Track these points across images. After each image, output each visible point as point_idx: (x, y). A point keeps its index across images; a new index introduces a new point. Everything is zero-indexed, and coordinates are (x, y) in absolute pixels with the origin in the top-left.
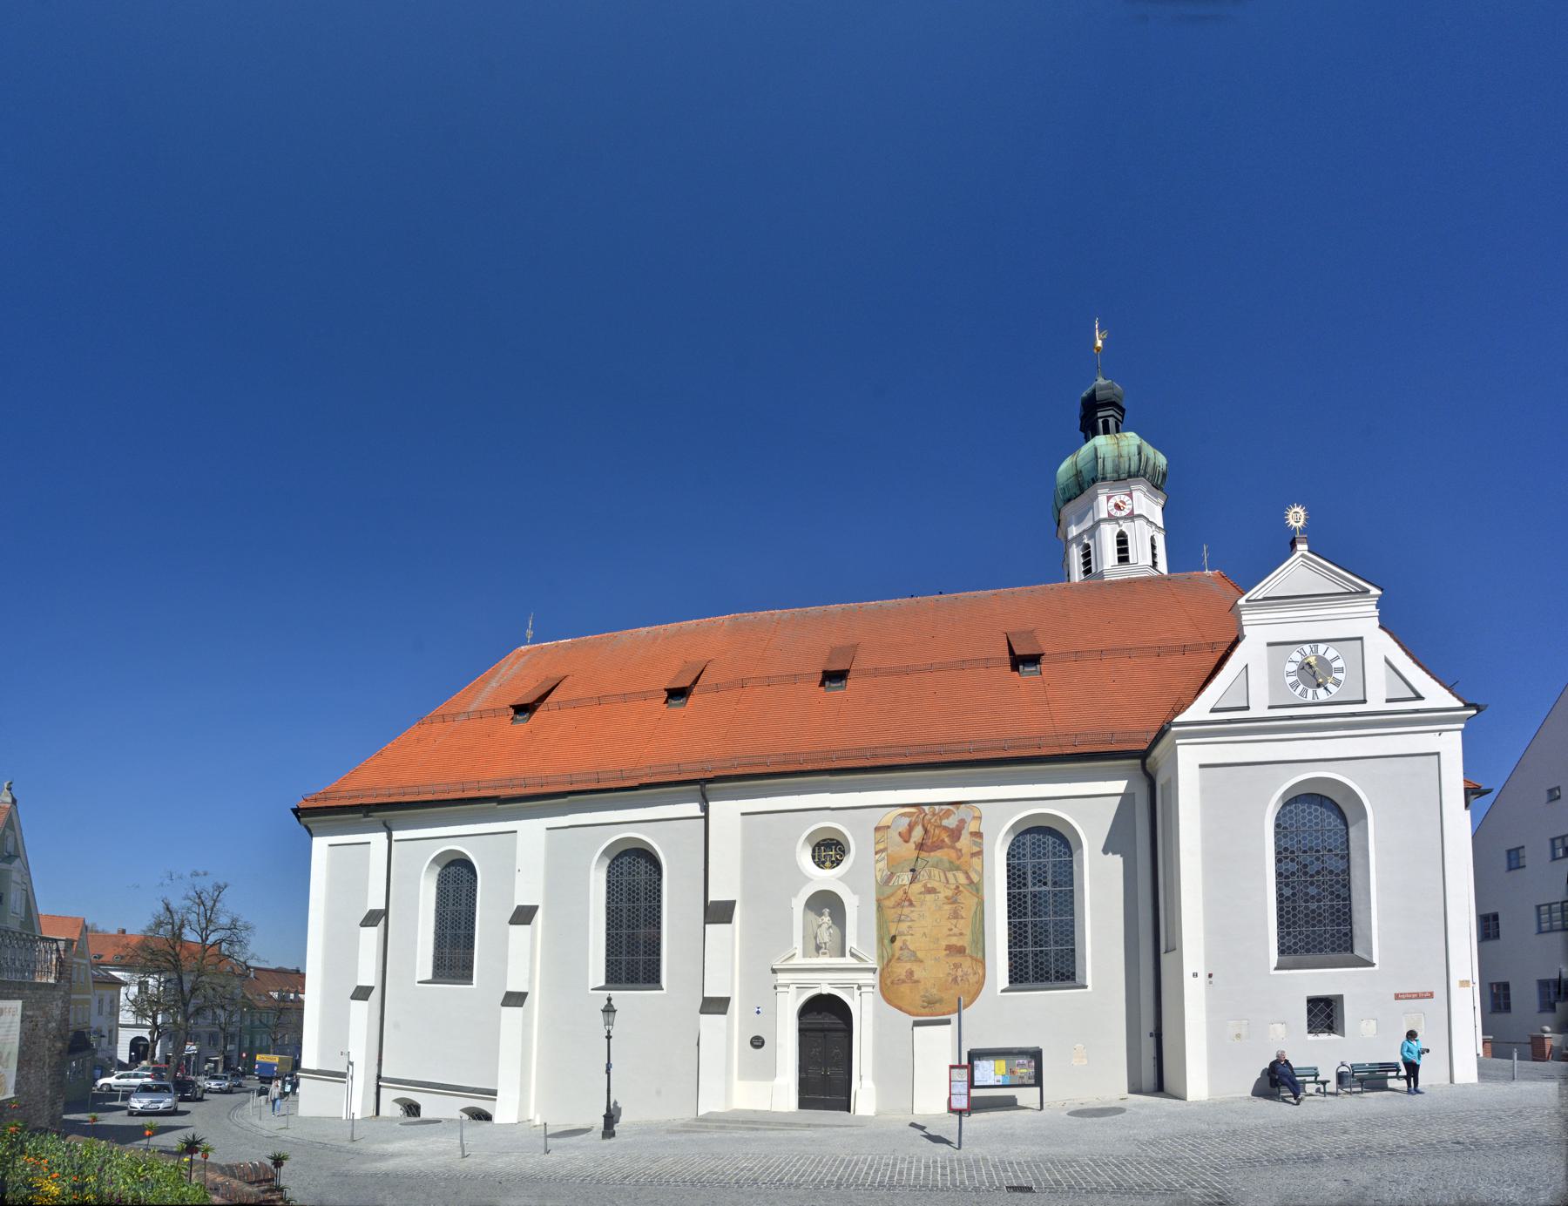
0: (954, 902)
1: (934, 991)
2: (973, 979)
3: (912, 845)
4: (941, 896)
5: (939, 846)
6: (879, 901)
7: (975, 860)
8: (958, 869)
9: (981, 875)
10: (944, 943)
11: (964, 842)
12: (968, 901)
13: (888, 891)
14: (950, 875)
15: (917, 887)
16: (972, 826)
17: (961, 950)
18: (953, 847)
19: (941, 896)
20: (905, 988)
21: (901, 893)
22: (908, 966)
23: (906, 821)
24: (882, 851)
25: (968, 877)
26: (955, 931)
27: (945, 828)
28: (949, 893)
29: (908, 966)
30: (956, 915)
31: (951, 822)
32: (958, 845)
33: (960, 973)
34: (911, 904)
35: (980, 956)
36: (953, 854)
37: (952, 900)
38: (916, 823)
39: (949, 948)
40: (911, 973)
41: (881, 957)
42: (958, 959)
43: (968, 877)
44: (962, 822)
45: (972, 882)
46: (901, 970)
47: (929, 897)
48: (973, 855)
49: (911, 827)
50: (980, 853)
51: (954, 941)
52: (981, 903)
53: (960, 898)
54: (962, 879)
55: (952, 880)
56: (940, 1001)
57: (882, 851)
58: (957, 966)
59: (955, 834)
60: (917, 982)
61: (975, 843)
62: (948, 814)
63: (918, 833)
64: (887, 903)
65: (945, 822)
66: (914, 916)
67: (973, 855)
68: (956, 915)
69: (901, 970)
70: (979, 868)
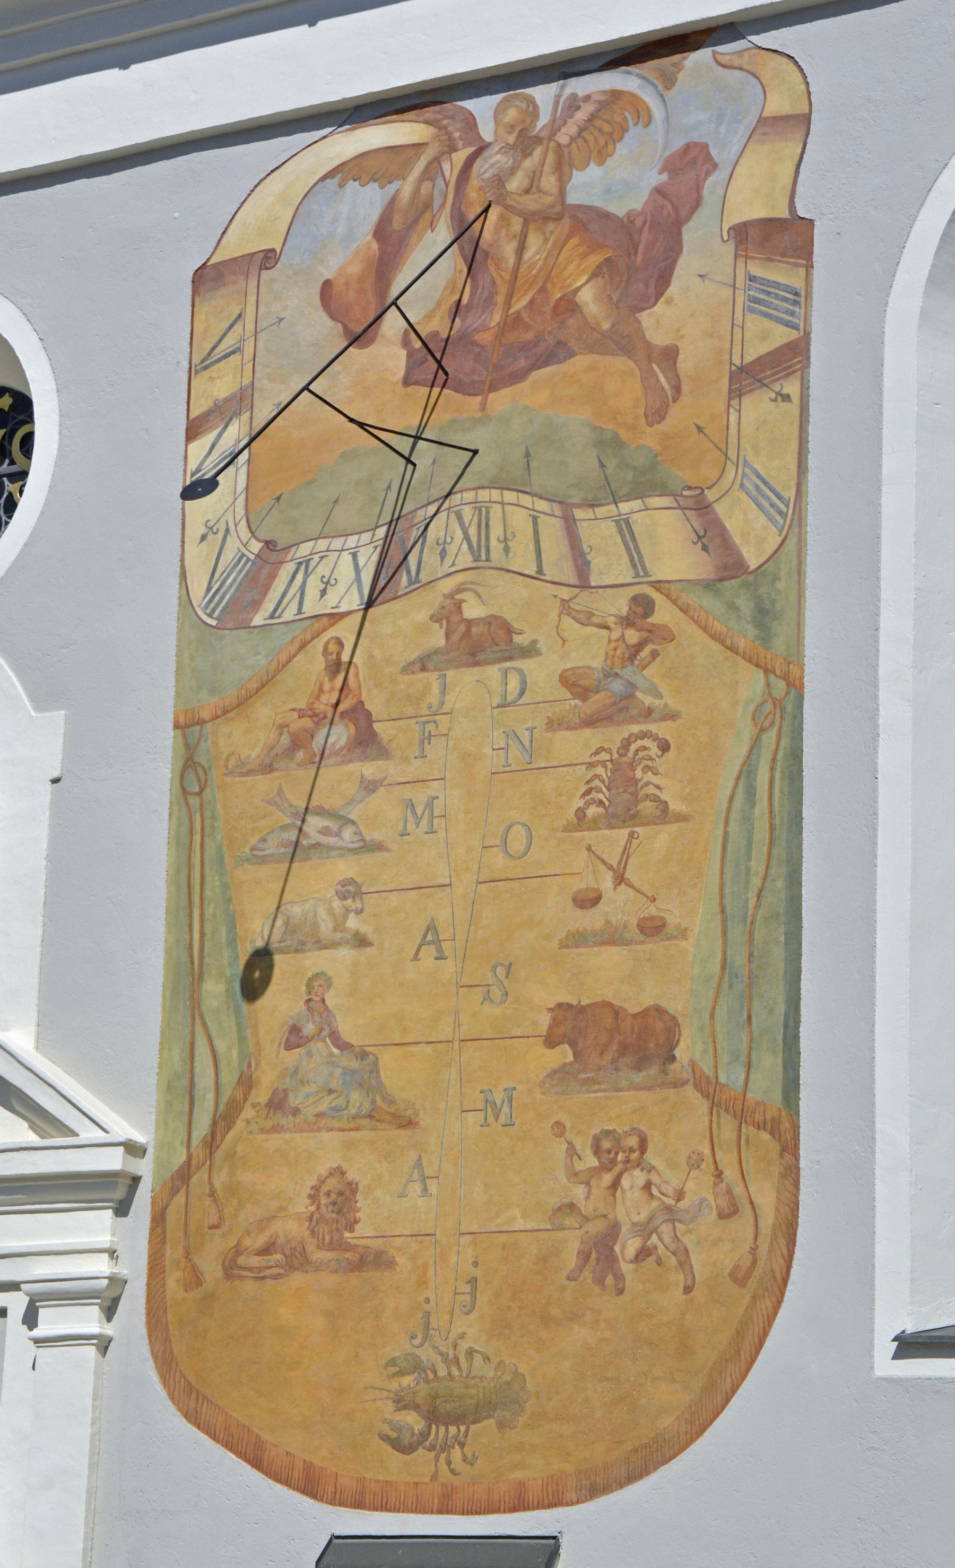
0: (621, 708)
1: (470, 1330)
2: (715, 1249)
3: (389, 354)
4: (541, 673)
5: (537, 346)
6: (187, 725)
7: (757, 408)
8: (646, 484)
9: (792, 516)
10: (544, 993)
11: (699, 303)
12: (704, 689)
13: (244, 657)
14: (597, 530)
15: (407, 624)
18: (626, 342)
19: (541, 673)
20: (298, 1305)
21: (313, 664)
22: (327, 1151)
23: (366, 203)
24: (223, 412)
25: (711, 535)
26: (619, 906)
27: (587, 223)
28: (589, 650)
29: (327, 1151)
30: (623, 800)
31: (617, 182)
32: (657, 324)
33: (632, 1207)
34: (366, 741)
35: (764, 1087)
36: (621, 380)
37: (599, 700)
38: (421, 212)
39: (572, 1025)
40: (339, 1200)
41: (180, 1092)
42: (624, 1105)
43: (711, 535)
44: (691, 162)
45: (731, 567)
46: (281, 1177)
47: (469, 686)
48: (748, 377)
49: (391, 239)
50: (792, 357)
51: (612, 978)
52: (783, 711)
53: (654, 681)
54: (672, 550)
55: (609, 566)
56: (499, 1402)
57: (223, 412)
58: (618, 1155)
59: (642, 252)
60: (372, 1261)
61: (762, 297)
62: (606, 127)
63: (428, 283)
64: (246, 738)
65: (587, 186)
66: (381, 814)
67: (748, 377)
68: (623, 800)
69: (281, 1177)
70: (780, 470)
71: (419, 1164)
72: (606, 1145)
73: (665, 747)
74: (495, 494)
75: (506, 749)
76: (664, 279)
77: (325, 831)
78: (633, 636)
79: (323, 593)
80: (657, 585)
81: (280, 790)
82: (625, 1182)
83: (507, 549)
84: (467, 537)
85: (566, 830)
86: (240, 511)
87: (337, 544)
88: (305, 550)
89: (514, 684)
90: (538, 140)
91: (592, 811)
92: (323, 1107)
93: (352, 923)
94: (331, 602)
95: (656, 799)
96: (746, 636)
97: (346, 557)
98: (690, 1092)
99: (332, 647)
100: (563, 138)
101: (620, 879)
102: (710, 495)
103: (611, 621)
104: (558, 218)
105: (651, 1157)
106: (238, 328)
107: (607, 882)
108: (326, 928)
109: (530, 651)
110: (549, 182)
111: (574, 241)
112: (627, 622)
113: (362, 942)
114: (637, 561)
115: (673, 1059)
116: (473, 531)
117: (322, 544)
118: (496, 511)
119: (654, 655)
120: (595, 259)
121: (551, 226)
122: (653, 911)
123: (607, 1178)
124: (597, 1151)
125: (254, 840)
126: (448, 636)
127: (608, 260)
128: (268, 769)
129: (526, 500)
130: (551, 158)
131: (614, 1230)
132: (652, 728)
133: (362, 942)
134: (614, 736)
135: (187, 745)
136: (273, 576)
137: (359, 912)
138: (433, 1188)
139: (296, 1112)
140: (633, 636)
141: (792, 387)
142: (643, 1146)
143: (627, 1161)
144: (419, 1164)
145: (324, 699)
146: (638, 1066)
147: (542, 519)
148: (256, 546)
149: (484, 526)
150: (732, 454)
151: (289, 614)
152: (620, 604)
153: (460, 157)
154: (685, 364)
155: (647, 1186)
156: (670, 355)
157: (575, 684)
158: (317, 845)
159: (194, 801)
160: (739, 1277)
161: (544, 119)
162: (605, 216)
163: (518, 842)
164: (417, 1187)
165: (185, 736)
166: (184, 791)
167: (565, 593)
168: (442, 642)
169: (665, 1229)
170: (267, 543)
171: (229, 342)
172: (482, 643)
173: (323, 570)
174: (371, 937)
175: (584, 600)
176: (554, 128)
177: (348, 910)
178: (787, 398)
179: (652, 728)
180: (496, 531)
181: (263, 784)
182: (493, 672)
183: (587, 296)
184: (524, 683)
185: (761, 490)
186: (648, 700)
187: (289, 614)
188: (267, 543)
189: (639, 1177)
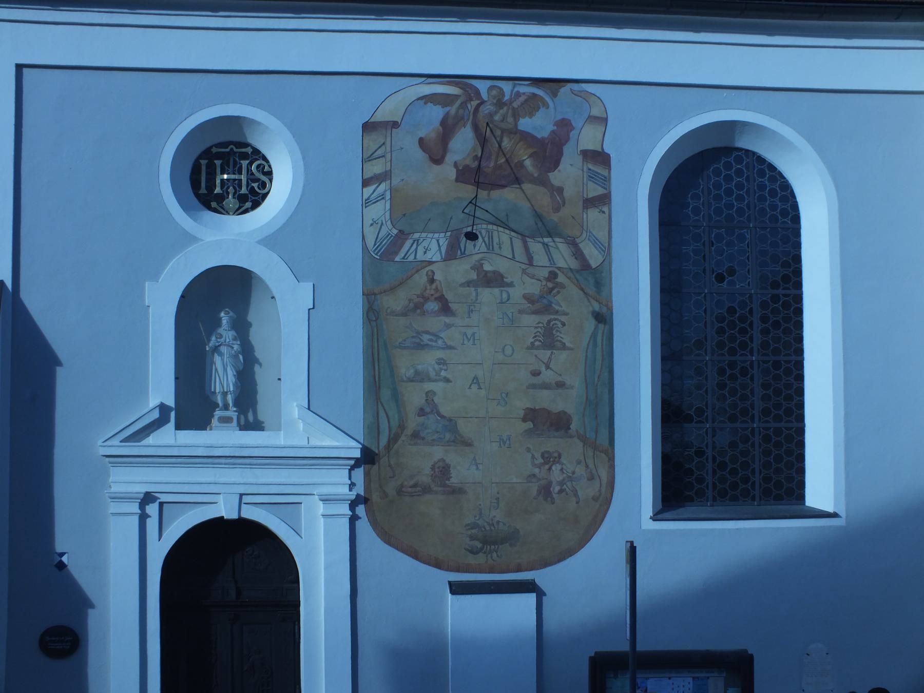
7: (593, 214)
16: (587, 138)
17: (558, 423)
18: (543, 182)
27: (527, 138)
37: (541, 304)
39: (531, 415)
42: (552, 443)
43: (578, 254)
45: (585, 266)
47: (488, 295)
48: (590, 203)
50: (604, 200)
54: (563, 257)
55: (540, 258)
58: (550, 459)
59: (550, 151)
65: (525, 124)
67: (590, 203)
71: (474, 459)
72: (546, 455)
73: (564, 324)
74: (495, 227)
75: (503, 318)
76: (557, 164)
77: (430, 340)
78: (550, 285)
79: (425, 253)
80: (559, 268)
81: (410, 324)
82: (554, 468)
83: (500, 248)
84: (484, 241)
85: (528, 348)
86: (388, 217)
87: (430, 235)
88: (416, 236)
89: (505, 296)
90: (505, 104)
91: (537, 343)
92: (435, 437)
93: (443, 373)
94: (428, 257)
95: (561, 342)
96: (591, 290)
97: (434, 241)
98: (576, 440)
99: (430, 273)
100: (515, 105)
101: (548, 367)
102: (577, 241)
103: (542, 278)
104: (515, 134)
105: (563, 460)
106: (383, 147)
107: (543, 368)
108: (432, 374)
109: (511, 285)
110: (510, 119)
111: (521, 143)
112: (548, 279)
113: (447, 380)
114: (551, 259)
115: (570, 429)
116: (486, 239)
117: (424, 235)
118: (495, 234)
119: (558, 292)
120: (531, 151)
121: (512, 136)
122: (560, 379)
123: (547, 467)
124: (543, 457)
125: (400, 340)
126: (478, 275)
127: (535, 152)
128: (404, 314)
129: (508, 232)
130: (510, 111)
131: (550, 484)
132: (559, 317)
133: (447, 380)
134: (545, 318)
135: (369, 302)
136: (403, 243)
137: (446, 370)
138: (480, 467)
139: (423, 439)
140: (550, 285)
141: (605, 209)
142: (560, 456)
143: (554, 461)
144: (474, 459)
145: (428, 292)
146: (557, 430)
147: (514, 239)
148: (395, 231)
149: (491, 238)
150: (585, 228)
151: (411, 258)
152: (545, 273)
153: (475, 103)
154: (567, 193)
155: (562, 470)
156: (560, 190)
157: (528, 298)
158: (427, 345)
159: (374, 324)
160: (595, 499)
161: (507, 97)
162: (533, 137)
163: (508, 351)
164: (474, 467)
165: (368, 299)
166: (370, 321)
167: (524, 266)
168: (475, 277)
169: (569, 484)
170: (400, 231)
171: (379, 152)
172: (493, 280)
173: (425, 244)
174: (451, 379)
175: (531, 270)
176: (511, 101)
177: (441, 369)
178: (604, 212)
179: (559, 317)
180: (496, 240)
181: (402, 321)
182: (496, 291)
183: (528, 163)
184: (509, 296)
185: (596, 242)
186: (557, 308)
187: (411, 258)
188: (400, 231)
189: (559, 467)
